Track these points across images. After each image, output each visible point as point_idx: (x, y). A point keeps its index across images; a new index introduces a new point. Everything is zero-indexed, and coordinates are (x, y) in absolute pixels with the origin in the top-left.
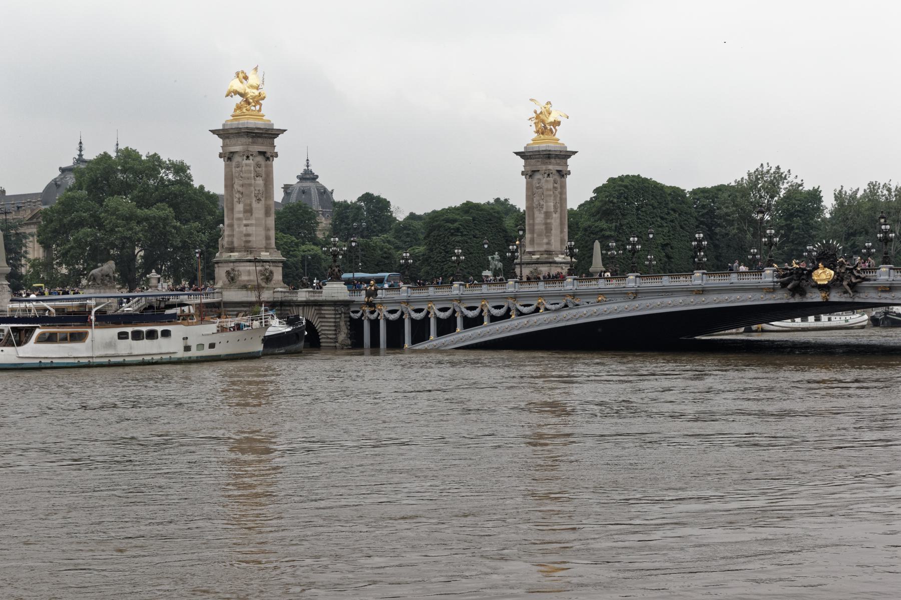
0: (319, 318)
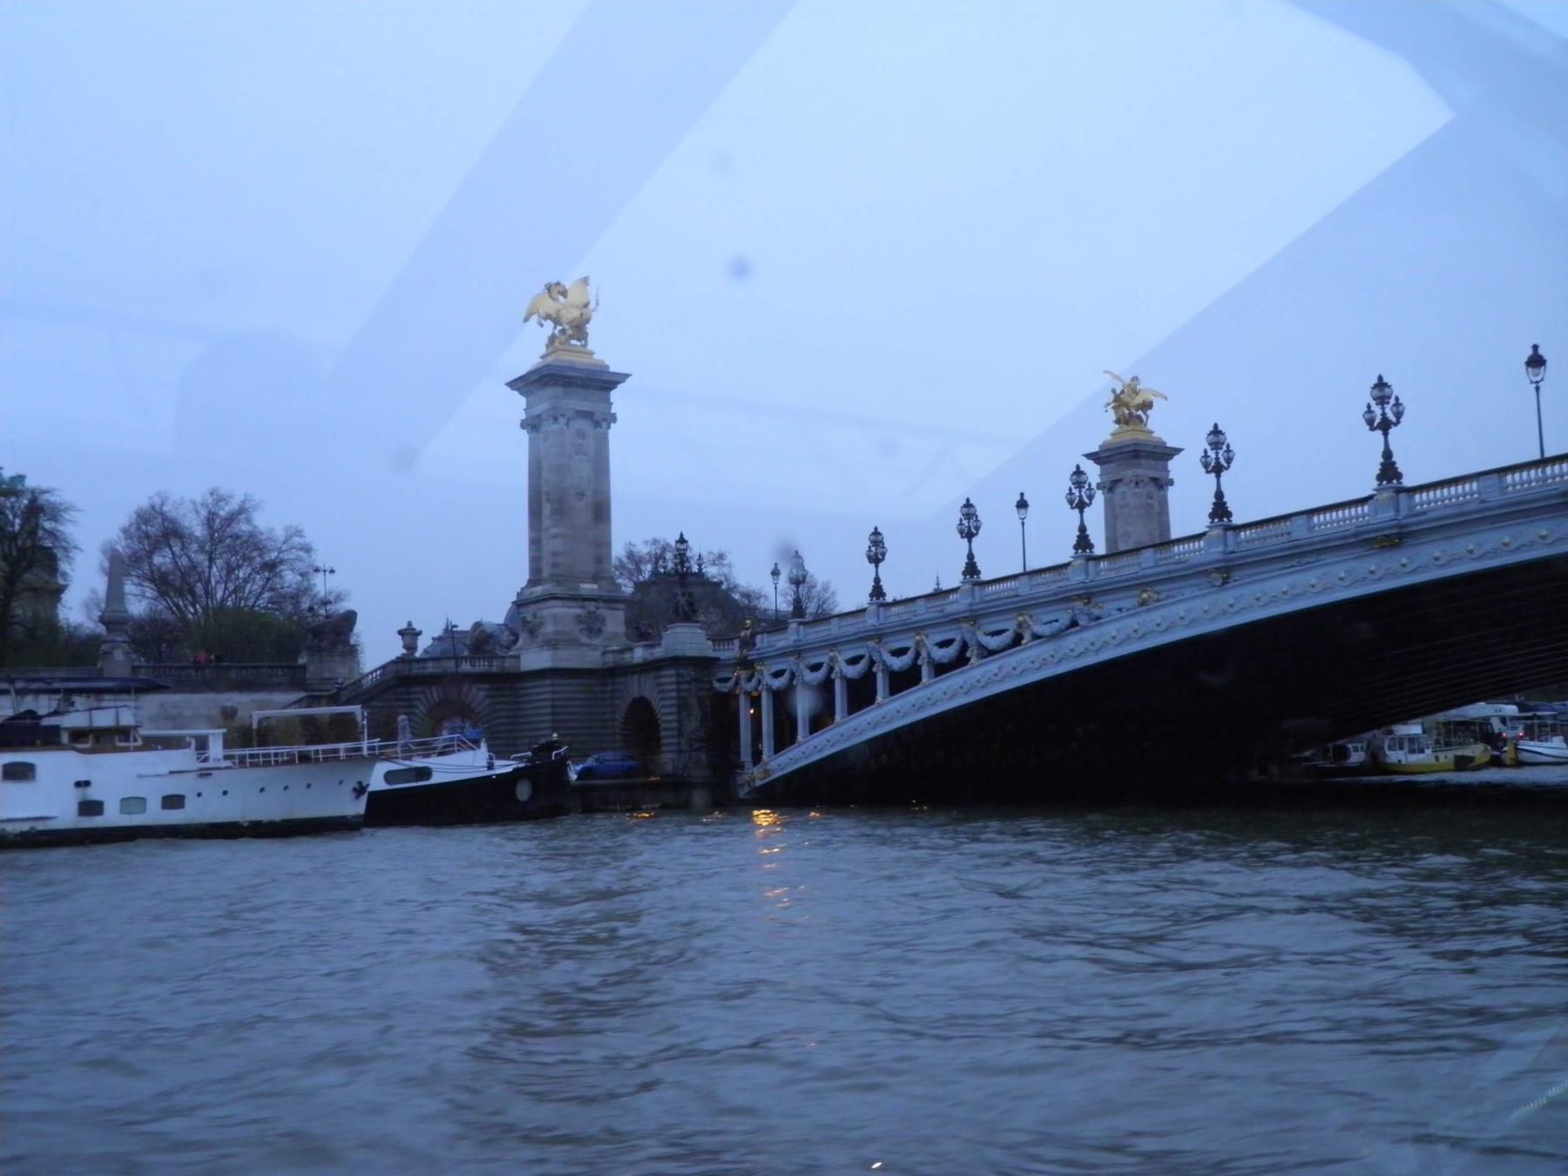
0: (659, 692)
